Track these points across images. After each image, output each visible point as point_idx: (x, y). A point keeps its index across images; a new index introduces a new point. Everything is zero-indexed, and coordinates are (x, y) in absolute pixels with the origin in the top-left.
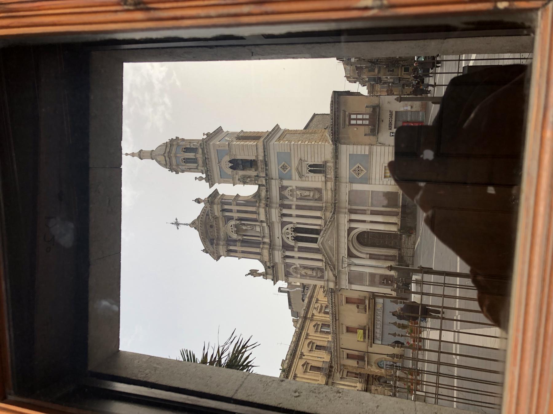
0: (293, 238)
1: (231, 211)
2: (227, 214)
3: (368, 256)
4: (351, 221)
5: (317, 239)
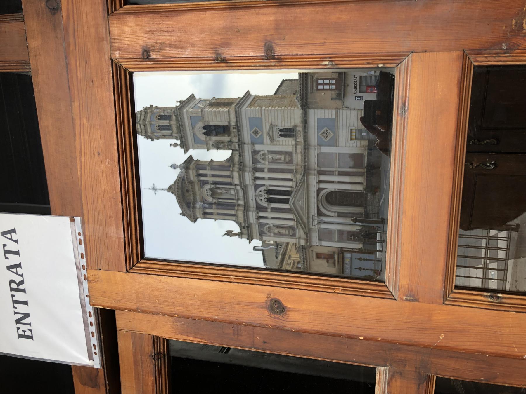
0: (266, 200)
1: (205, 175)
2: (202, 178)
3: (336, 214)
4: (320, 182)
5: (288, 200)
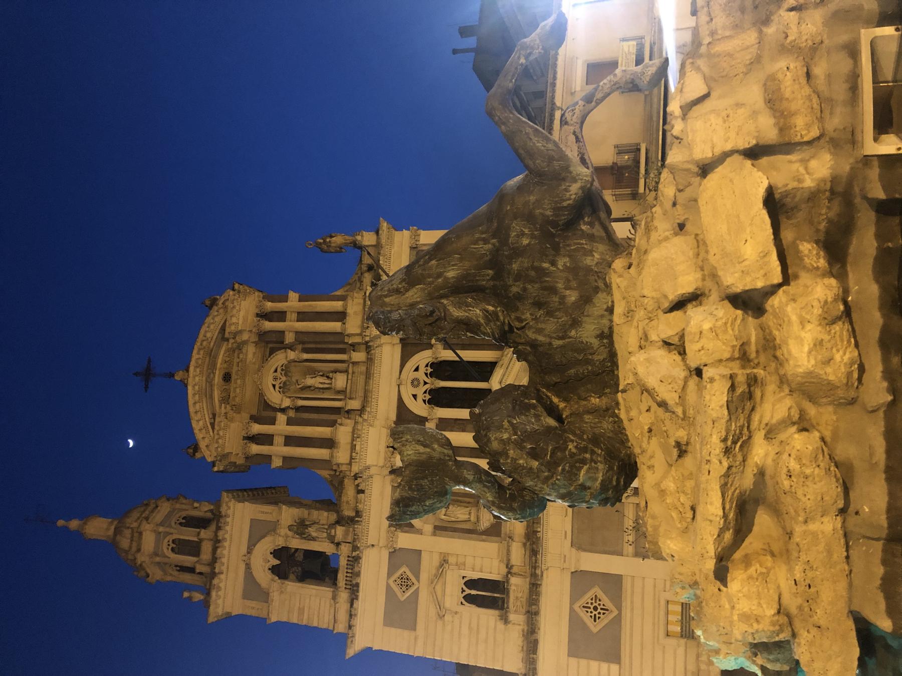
0: (428, 397)
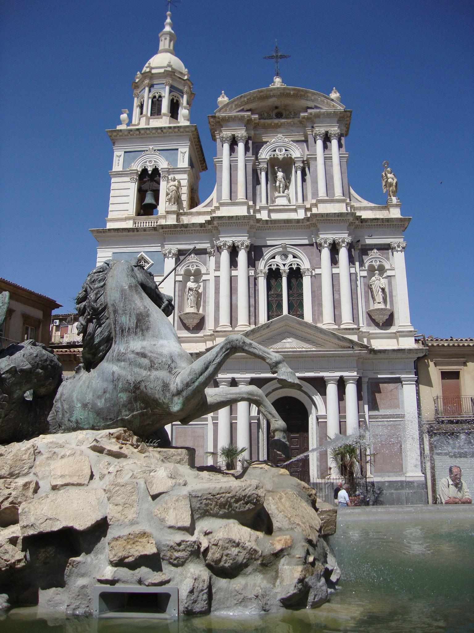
4: (341, 384)
